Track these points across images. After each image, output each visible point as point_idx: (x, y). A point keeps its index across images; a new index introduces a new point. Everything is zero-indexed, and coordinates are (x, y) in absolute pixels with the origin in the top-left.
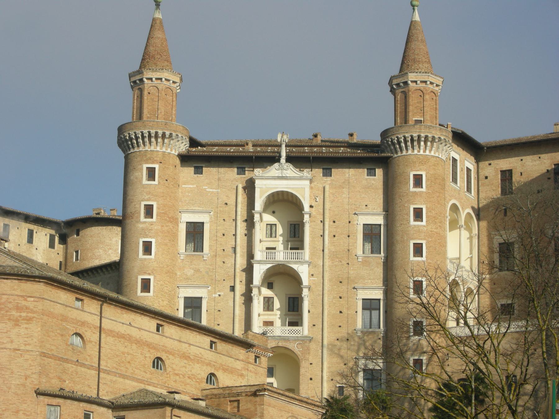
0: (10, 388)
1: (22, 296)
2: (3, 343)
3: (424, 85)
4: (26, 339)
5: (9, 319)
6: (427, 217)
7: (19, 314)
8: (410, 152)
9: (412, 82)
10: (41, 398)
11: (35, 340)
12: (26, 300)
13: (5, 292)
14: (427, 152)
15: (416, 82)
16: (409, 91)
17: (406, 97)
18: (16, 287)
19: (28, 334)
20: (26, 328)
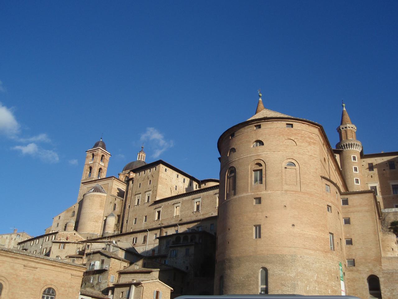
0: (310, 173)
1: (310, 132)
2: (305, 152)
3: (352, 128)
4: (314, 152)
5: (306, 142)
6: (359, 170)
7: (310, 140)
8: (350, 149)
9: (348, 127)
10: (323, 180)
11: (318, 153)
12: (312, 135)
13: (303, 130)
14: (356, 150)
15: (349, 127)
16: (347, 130)
17: (346, 132)
18: (307, 128)
19: (314, 150)
20: (314, 147)
